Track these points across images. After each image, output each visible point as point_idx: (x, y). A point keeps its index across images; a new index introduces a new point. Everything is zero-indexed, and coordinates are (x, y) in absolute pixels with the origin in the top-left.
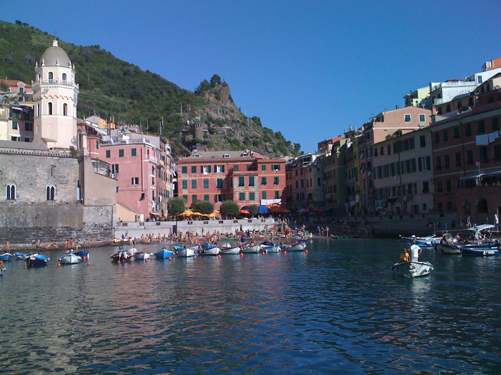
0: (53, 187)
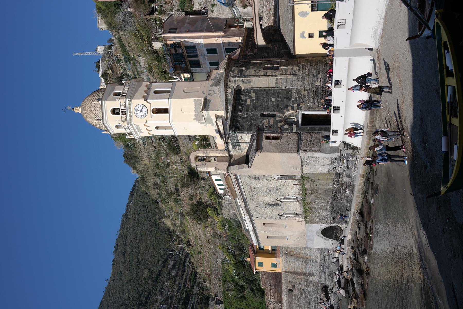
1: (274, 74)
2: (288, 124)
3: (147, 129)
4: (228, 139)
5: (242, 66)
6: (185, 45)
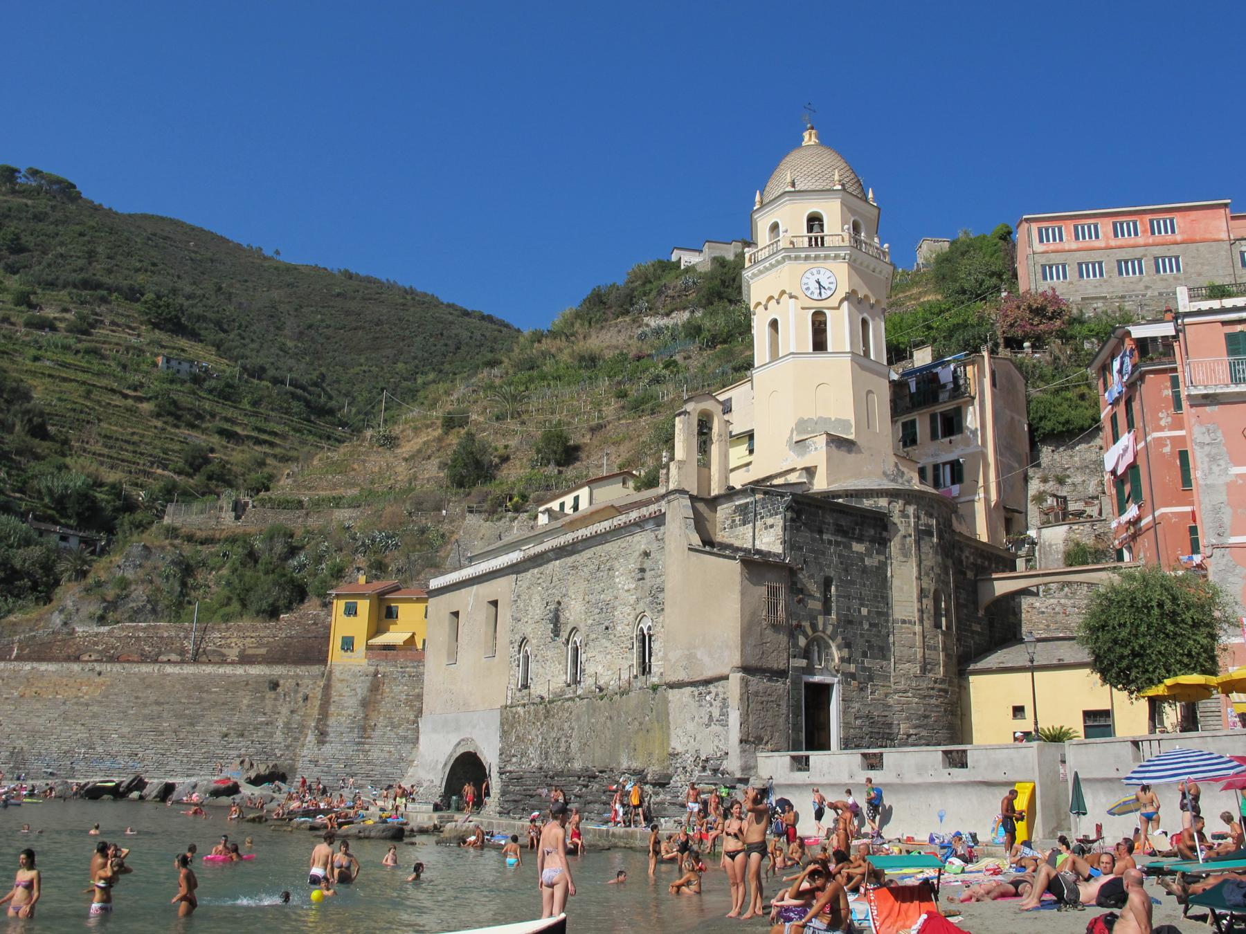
0: (649, 628)
1: (925, 616)
2: (808, 645)
3: (771, 298)
4: (765, 493)
5: (940, 537)
6: (963, 409)
